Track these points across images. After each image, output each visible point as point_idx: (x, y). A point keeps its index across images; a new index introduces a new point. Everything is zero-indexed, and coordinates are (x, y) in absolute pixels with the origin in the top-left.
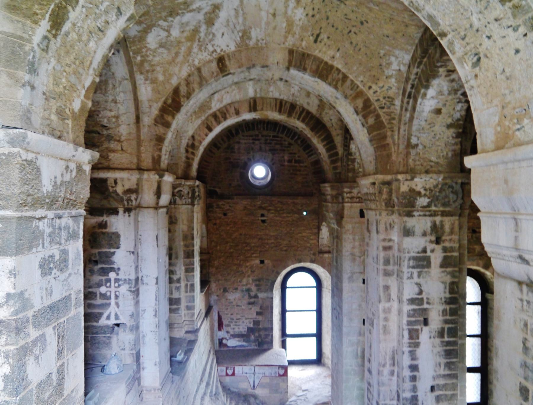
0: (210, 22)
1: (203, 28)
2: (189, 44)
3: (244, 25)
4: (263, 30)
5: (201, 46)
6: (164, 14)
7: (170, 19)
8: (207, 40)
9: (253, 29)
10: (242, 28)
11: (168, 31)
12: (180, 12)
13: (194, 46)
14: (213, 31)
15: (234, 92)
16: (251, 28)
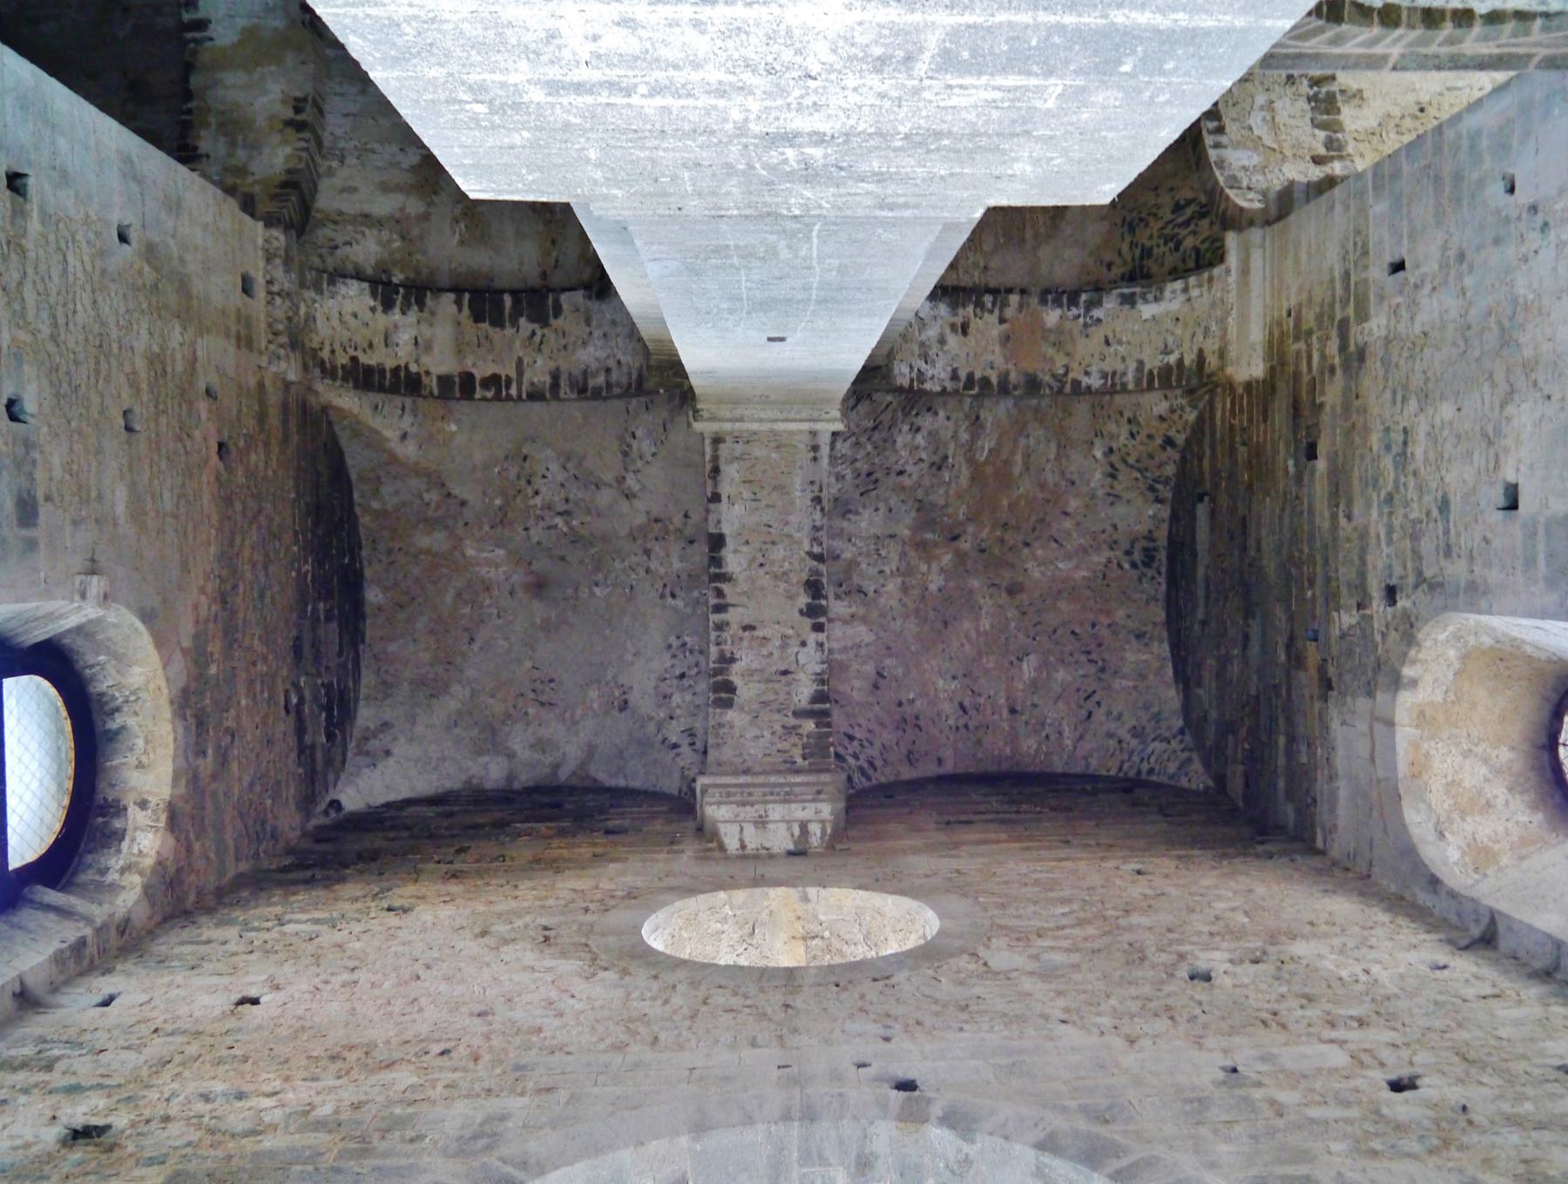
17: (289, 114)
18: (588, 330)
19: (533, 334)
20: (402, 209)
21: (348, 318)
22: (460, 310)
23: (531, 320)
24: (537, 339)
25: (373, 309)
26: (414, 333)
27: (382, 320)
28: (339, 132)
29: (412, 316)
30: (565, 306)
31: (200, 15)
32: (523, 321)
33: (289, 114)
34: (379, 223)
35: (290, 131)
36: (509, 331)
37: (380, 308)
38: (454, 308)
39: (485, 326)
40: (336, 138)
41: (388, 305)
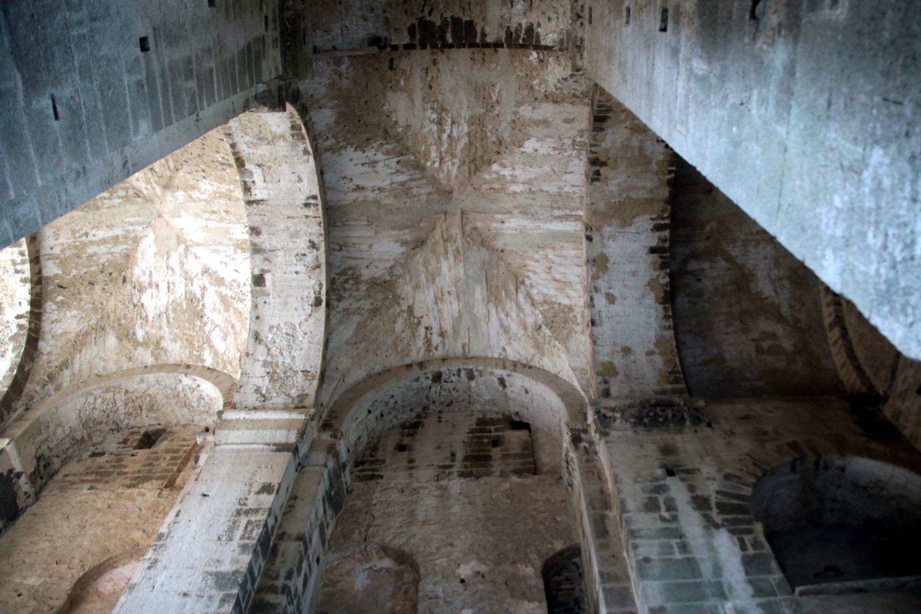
0: (220, 281)
1: (223, 290)
2: (231, 311)
3: (228, 245)
4: (231, 225)
5: (239, 298)
6: (198, 323)
7: (205, 319)
8: (236, 290)
9: (231, 236)
10: (232, 248)
11: (216, 326)
12: (200, 307)
13: (236, 306)
14: (230, 280)
15: (550, 256)
16: (230, 239)
17: (603, 170)
18: (387, 15)
19: (430, 13)
20: (534, 108)
21: (553, 16)
22: (483, 29)
23: (431, 24)
24: (427, 10)
25: (539, 25)
26: (514, 11)
27: (534, 18)
28: (576, 161)
29: (515, 22)
30: (406, 33)
31: (657, 234)
32: (438, 23)
33: (603, 170)
34: (547, 97)
35: (603, 158)
36: (448, 15)
37: (535, 27)
38: (488, 30)
39: (465, 19)
40: (578, 157)
41: (530, 29)
